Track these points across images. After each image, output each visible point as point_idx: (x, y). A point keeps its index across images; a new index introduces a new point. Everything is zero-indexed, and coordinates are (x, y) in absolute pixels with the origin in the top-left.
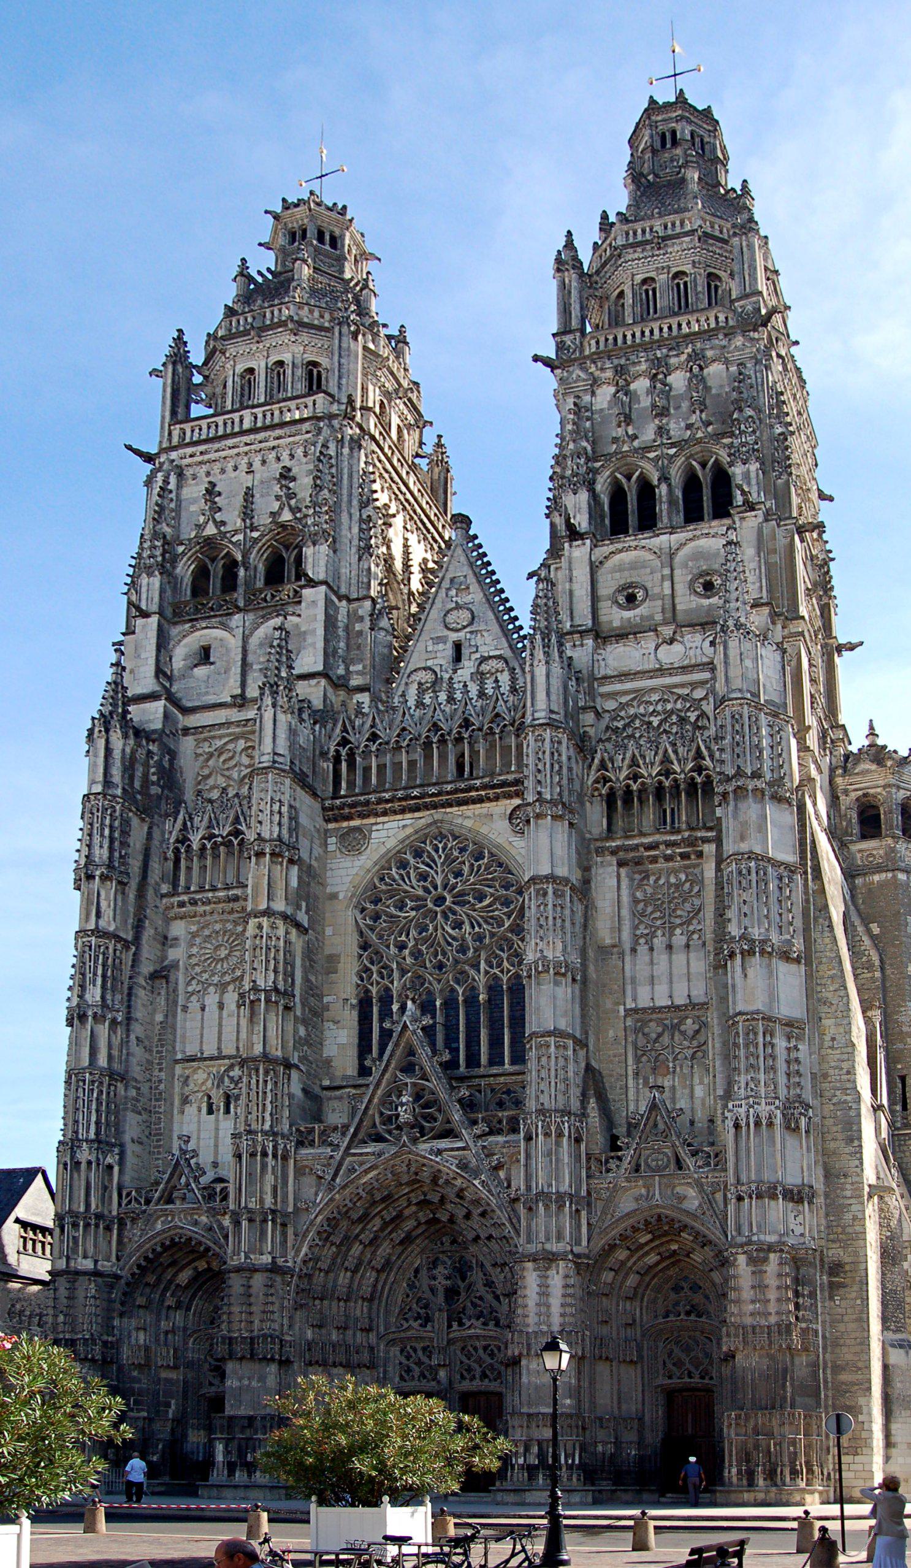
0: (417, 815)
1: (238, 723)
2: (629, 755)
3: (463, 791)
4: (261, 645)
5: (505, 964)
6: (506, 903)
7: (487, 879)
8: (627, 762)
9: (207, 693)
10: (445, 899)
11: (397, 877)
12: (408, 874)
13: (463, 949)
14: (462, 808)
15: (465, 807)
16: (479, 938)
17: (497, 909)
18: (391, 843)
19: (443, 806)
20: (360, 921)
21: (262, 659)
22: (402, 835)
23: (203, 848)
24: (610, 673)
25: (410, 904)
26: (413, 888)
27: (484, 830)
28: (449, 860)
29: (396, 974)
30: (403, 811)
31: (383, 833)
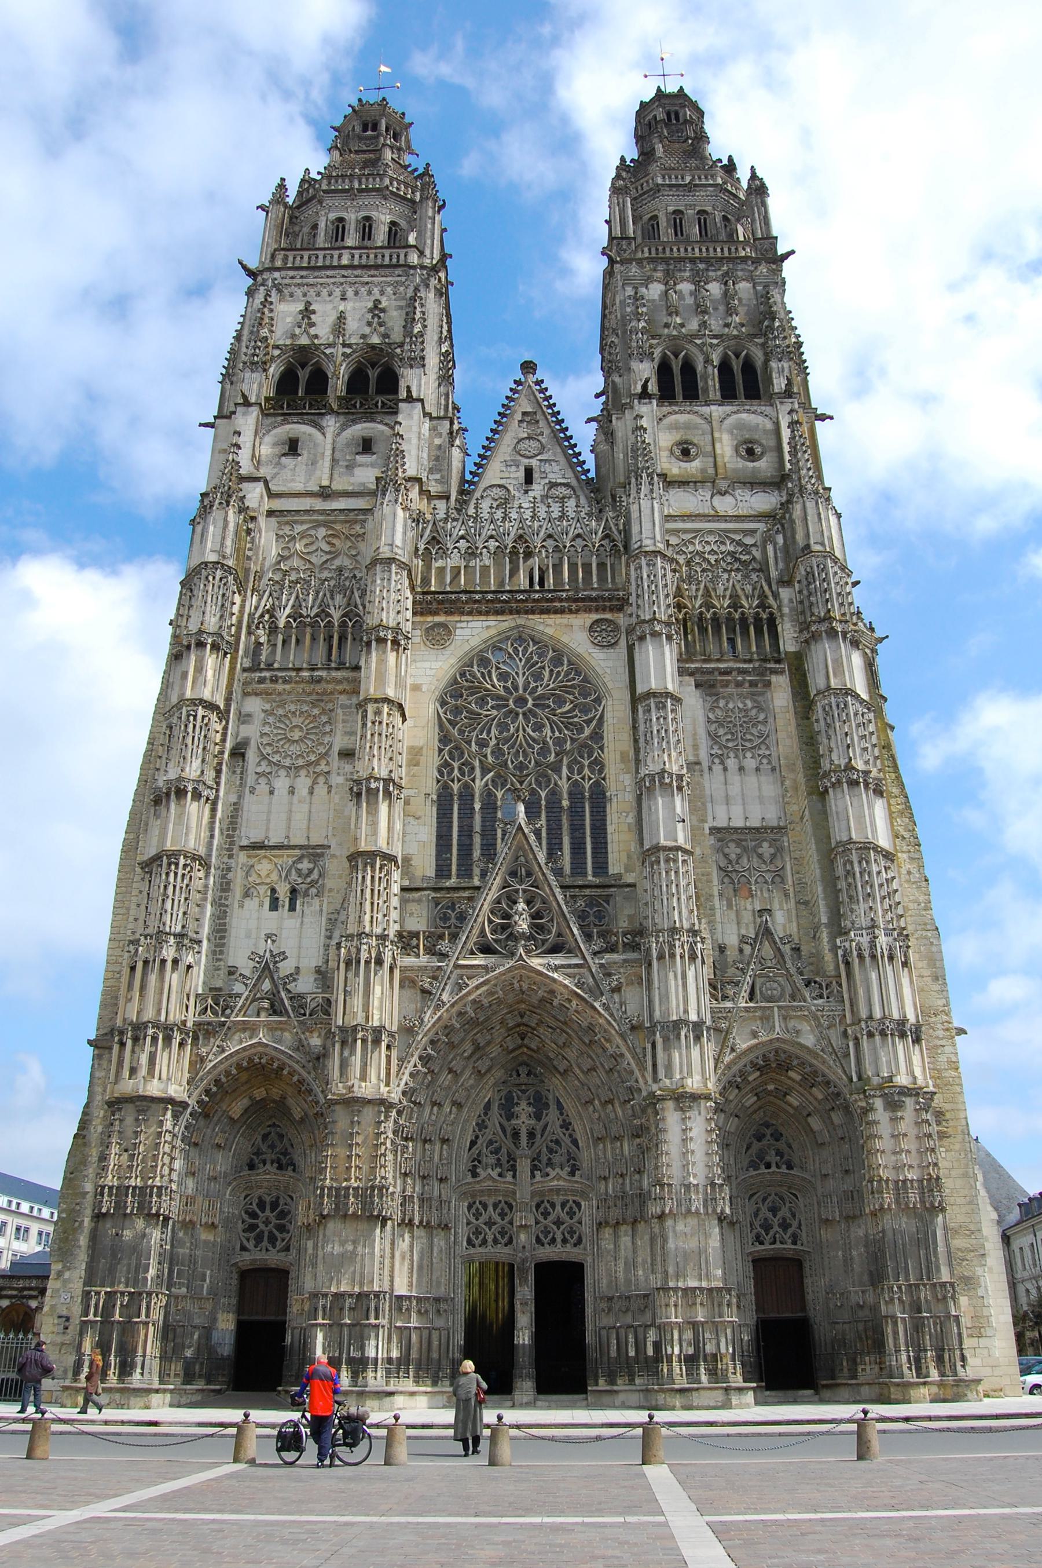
0: (500, 618)
1: (323, 512)
2: (702, 586)
3: (548, 600)
4: (348, 445)
5: (586, 771)
6: (585, 709)
7: (566, 686)
8: (700, 593)
9: (293, 480)
10: (526, 701)
11: (479, 675)
12: (490, 672)
13: (544, 751)
14: (543, 616)
15: (546, 616)
16: (559, 742)
17: (576, 716)
18: (475, 642)
19: (527, 612)
20: (442, 715)
21: (348, 457)
22: (486, 635)
23: (288, 624)
24: (673, 513)
25: (491, 703)
26: (493, 686)
27: (565, 639)
28: (530, 664)
29: (478, 772)
30: (487, 613)
31: (468, 632)
